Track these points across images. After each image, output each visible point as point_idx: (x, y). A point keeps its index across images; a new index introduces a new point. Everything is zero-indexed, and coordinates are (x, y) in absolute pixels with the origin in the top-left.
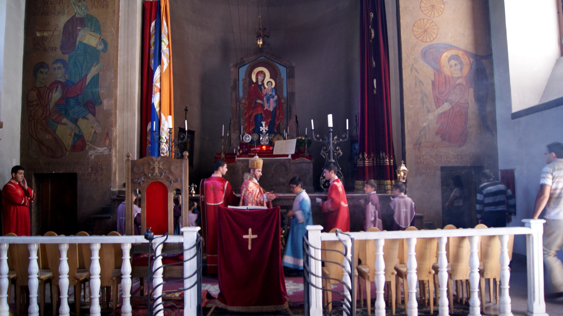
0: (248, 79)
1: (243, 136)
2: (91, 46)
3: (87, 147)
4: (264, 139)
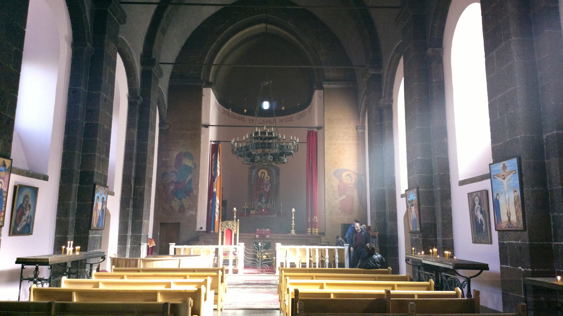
3: (186, 211)
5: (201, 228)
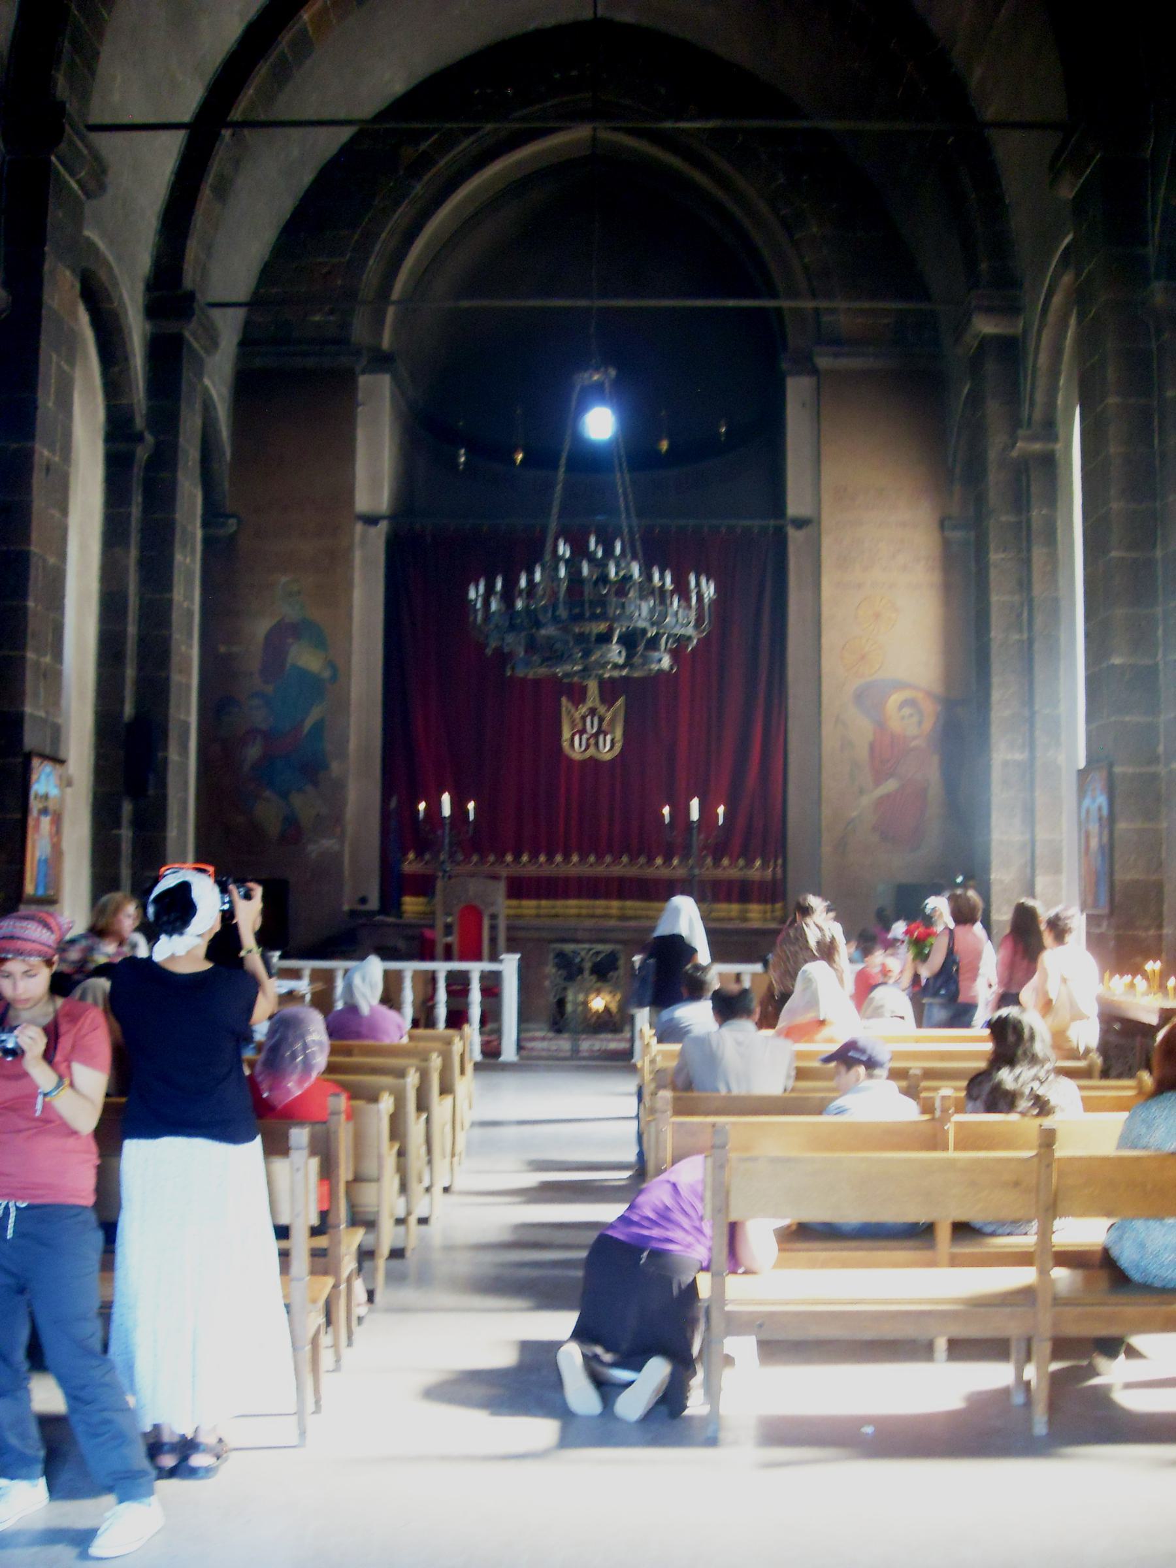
5: (363, 900)
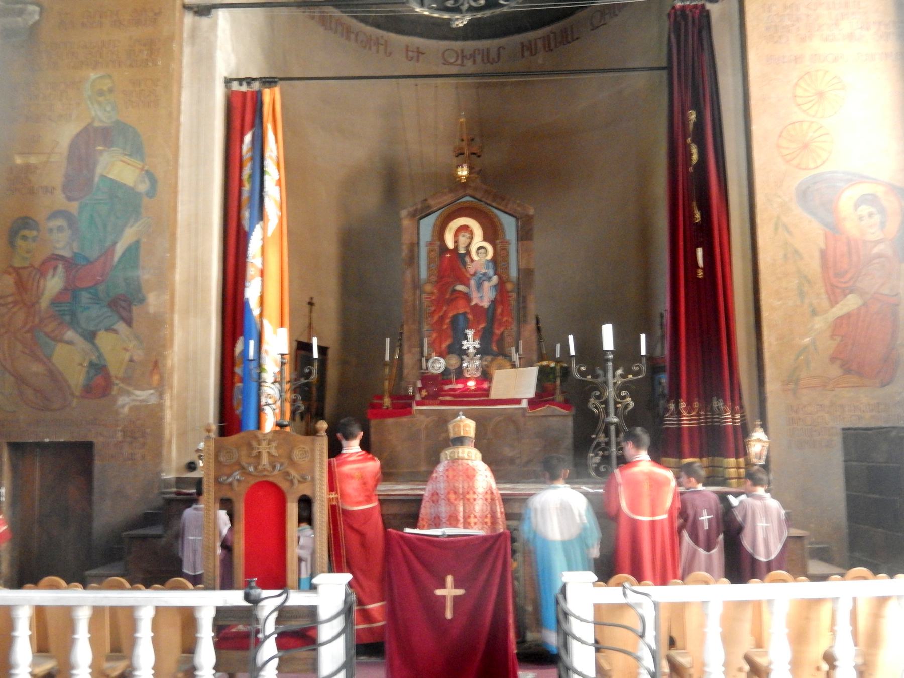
0: (438, 243)
1: (427, 360)
2: (125, 185)
3: (115, 388)
4: (472, 366)
